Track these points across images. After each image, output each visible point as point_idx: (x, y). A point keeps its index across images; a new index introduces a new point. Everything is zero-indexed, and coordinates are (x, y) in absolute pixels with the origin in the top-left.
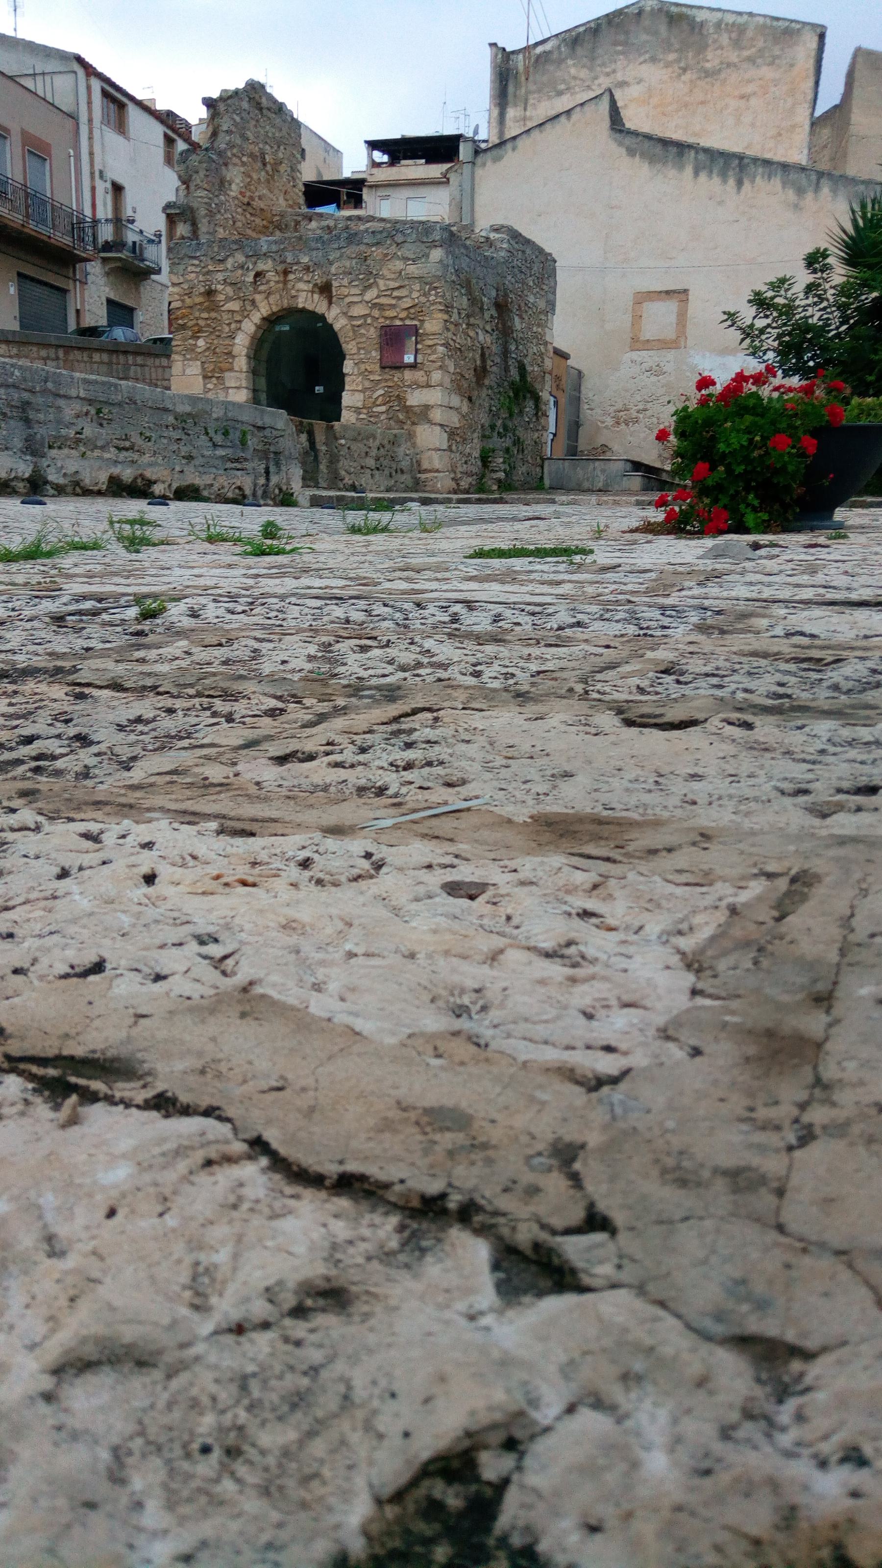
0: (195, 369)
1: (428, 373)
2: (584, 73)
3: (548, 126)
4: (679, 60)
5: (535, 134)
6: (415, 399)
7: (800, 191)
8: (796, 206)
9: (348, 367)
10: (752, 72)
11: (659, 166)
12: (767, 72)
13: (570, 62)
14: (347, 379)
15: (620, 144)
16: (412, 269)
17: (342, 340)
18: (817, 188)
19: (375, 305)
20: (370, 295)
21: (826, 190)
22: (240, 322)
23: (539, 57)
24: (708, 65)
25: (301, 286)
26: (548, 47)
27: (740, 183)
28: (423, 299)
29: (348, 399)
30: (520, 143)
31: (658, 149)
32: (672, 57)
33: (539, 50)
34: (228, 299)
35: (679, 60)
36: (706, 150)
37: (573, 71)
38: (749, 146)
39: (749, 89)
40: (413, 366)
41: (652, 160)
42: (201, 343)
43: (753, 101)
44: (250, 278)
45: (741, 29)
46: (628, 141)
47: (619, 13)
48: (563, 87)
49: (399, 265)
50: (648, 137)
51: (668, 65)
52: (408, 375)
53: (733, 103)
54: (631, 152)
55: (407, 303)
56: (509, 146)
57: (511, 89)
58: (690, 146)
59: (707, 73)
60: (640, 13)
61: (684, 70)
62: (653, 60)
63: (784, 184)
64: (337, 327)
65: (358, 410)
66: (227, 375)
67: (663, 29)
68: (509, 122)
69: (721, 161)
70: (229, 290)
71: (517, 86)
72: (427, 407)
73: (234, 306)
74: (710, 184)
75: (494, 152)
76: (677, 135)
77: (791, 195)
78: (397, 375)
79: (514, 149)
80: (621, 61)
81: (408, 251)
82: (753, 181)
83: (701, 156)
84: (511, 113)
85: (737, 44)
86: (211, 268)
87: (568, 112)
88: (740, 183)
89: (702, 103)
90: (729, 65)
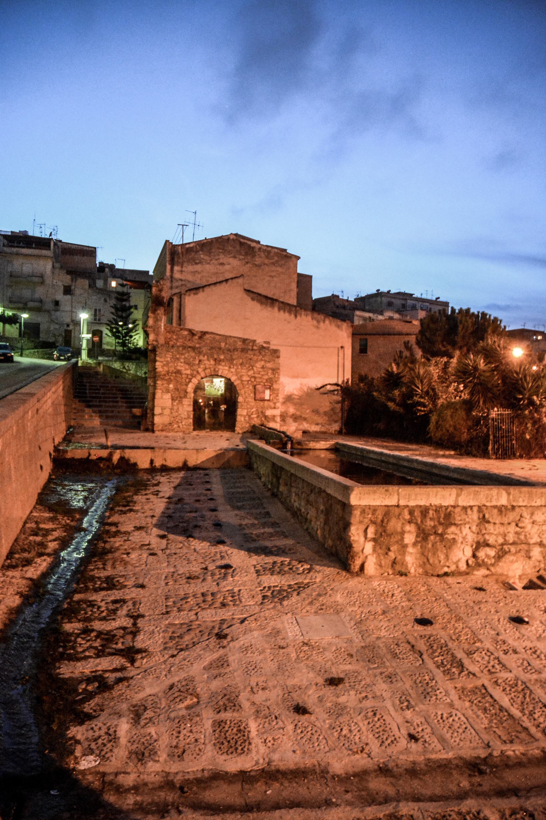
0: (168, 396)
1: (275, 403)
2: (206, 258)
3: (218, 284)
4: (244, 259)
5: (213, 287)
6: (269, 413)
7: (318, 322)
8: (318, 327)
9: (240, 399)
10: (274, 268)
11: (264, 306)
12: (279, 269)
13: (201, 253)
14: (239, 405)
15: (248, 296)
16: (269, 365)
17: (238, 389)
18: (324, 321)
19: (252, 377)
20: (251, 373)
21: (327, 322)
22: (191, 379)
23: (187, 249)
24: (256, 263)
25: (220, 367)
26: (191, 245)
27: (296, 316)
28: (272, 376)
29: (239, 411)
30: (206, 289)
31: (264, 300)
32: (241, 257)
33: (187, 246)
34: (186, 369)
35: (244, 259)
36: (283, 303)
37: (202, 256)
38: (274, 295)
39: (273, 274)
40: (269, 400)
41: (262, 303)
42: (171, 386)
43: (275, 279)
44: (197, 362)
45: (269, 252)
46: (252, 295)
47: (221, 237)
48: (197, 261)
49: (263, 363)
50: (260, 295)
51: (240, 260)
52: (266, 403)
53: (268, 278)
54: (253, 299)
55: (266, 377)
56: (201, 290)
57: (176, 259)
58: (276, 300)
59: (256, 265)
60: (229, 239)
61: (247, 263)
62: (235, 257)
63: (312, 319)
64: (235, 384)
65: (245, 417)
66: (184, 400)
67: (238, 247)
68: (175, 271)
69: (288, 307)
70: (187, 367)
71: (179, 258)
72: (274, 416)
73: (189, 372)
74: (285, 315)
75: (195, 291)
76: (270, 295)
77: (315, 322)
78: (262, 403)
79: (203, 291)
80: (222, 256)
81: (267, 358)
82: (301, 316)
83: (281, 305)
84: (176, 268)
85: (267, 257)
86: (178, 356)
87: (226, 281)
88: (296, 316)
89: (255, 276)
90: (264, 264)
